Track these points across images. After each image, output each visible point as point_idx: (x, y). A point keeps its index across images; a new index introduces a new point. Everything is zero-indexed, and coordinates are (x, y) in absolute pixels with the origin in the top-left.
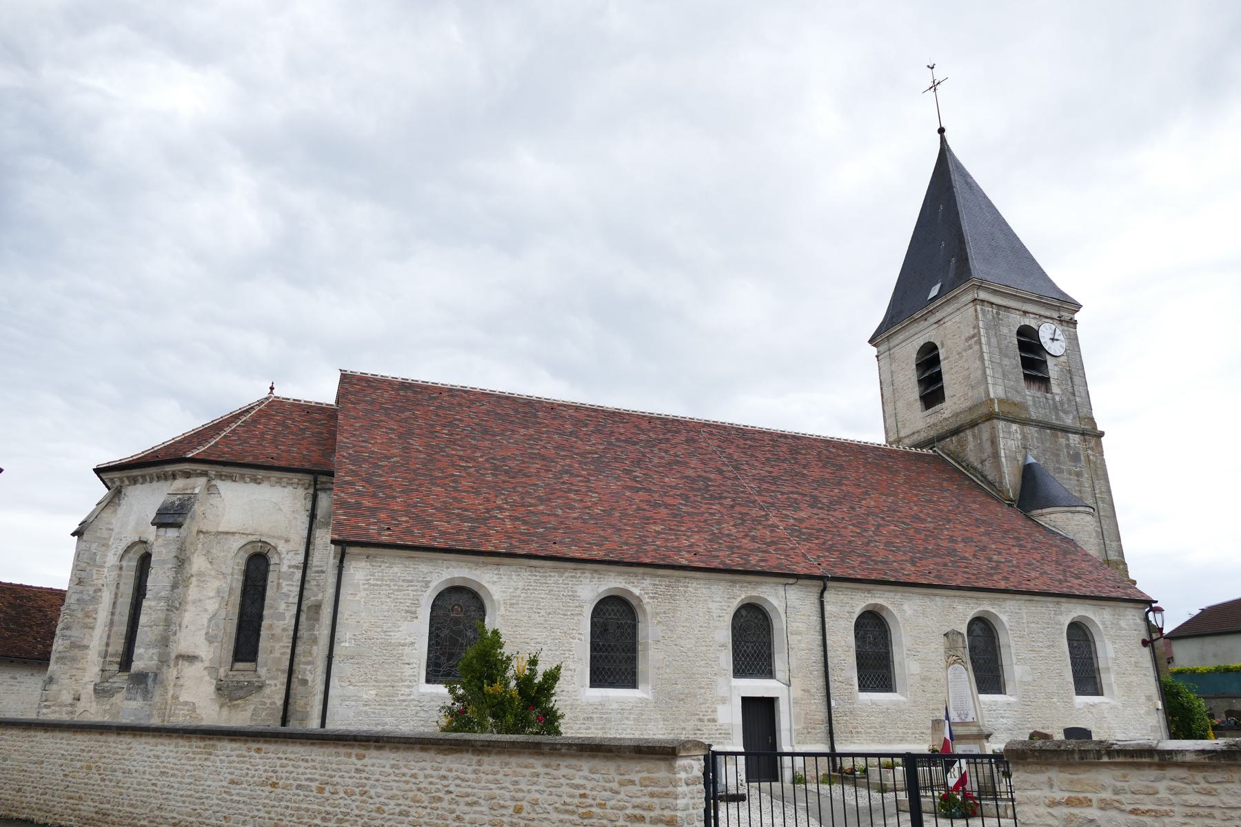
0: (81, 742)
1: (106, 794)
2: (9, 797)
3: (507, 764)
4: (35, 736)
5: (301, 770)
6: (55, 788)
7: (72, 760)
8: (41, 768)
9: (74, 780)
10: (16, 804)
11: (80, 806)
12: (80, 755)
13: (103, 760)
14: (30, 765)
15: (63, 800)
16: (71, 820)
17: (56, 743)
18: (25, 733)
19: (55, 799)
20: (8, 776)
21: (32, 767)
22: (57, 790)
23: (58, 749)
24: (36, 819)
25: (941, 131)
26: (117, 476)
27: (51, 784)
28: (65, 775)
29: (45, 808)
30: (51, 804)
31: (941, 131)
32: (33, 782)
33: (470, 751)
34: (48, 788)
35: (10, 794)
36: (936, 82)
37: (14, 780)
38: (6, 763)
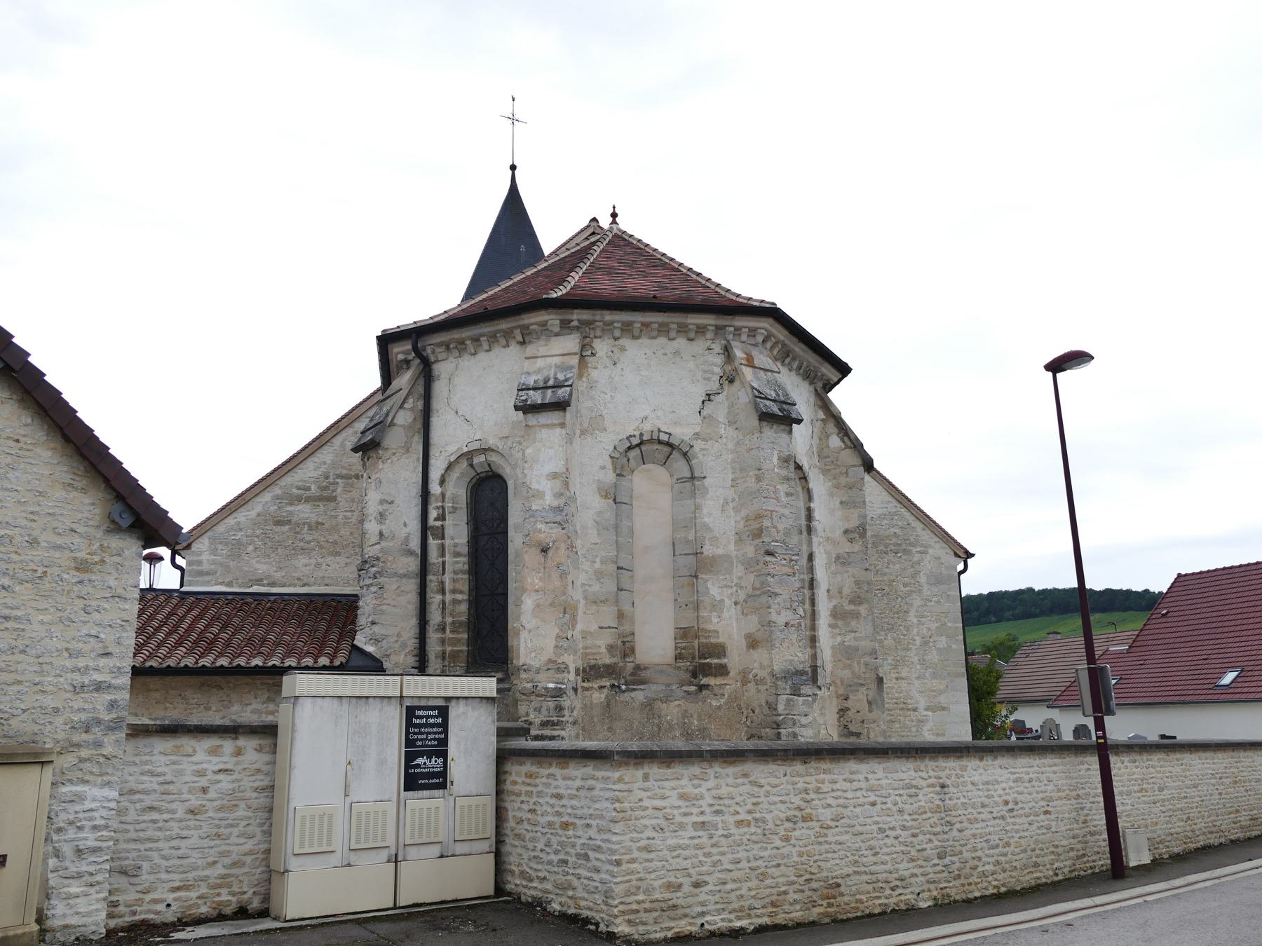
0: (1221, 760)
1: (1251, 802)
2: (1179, 830)
3: (1135, 761)
4: (1183, 759)
5: (525, 807)
6: (1217, 807)
7: (1221, 778)
8: (1199, 791)
9: (1228, 797)
10: (1190, 834)
11: (1239, 818)
12: (1225, 773)
13: (1242, 774)
14: (1188, 790)
15: (1226, 817)
16: (1237, 833)
17: (1204, 763)
18: (1080, 759)
19: (1220, 817)
20: (1171, 807)
21: (1192, 792)
22: (1219, 809)
23: (1206, 768)
24: (1212, 841)
25: (513, 168)
26: (713, 322)
27: (1212, 804)
28: (1220, 794)
29: (1214, 829)
30: (1218, 823)
31: (513, 168)
32: (1197, 807)
33: (554, 764)
34: (1211, 809)
35: (1179, 827)
36: (515, 122)
37: (1178, 809)
38: (1164, 792)
